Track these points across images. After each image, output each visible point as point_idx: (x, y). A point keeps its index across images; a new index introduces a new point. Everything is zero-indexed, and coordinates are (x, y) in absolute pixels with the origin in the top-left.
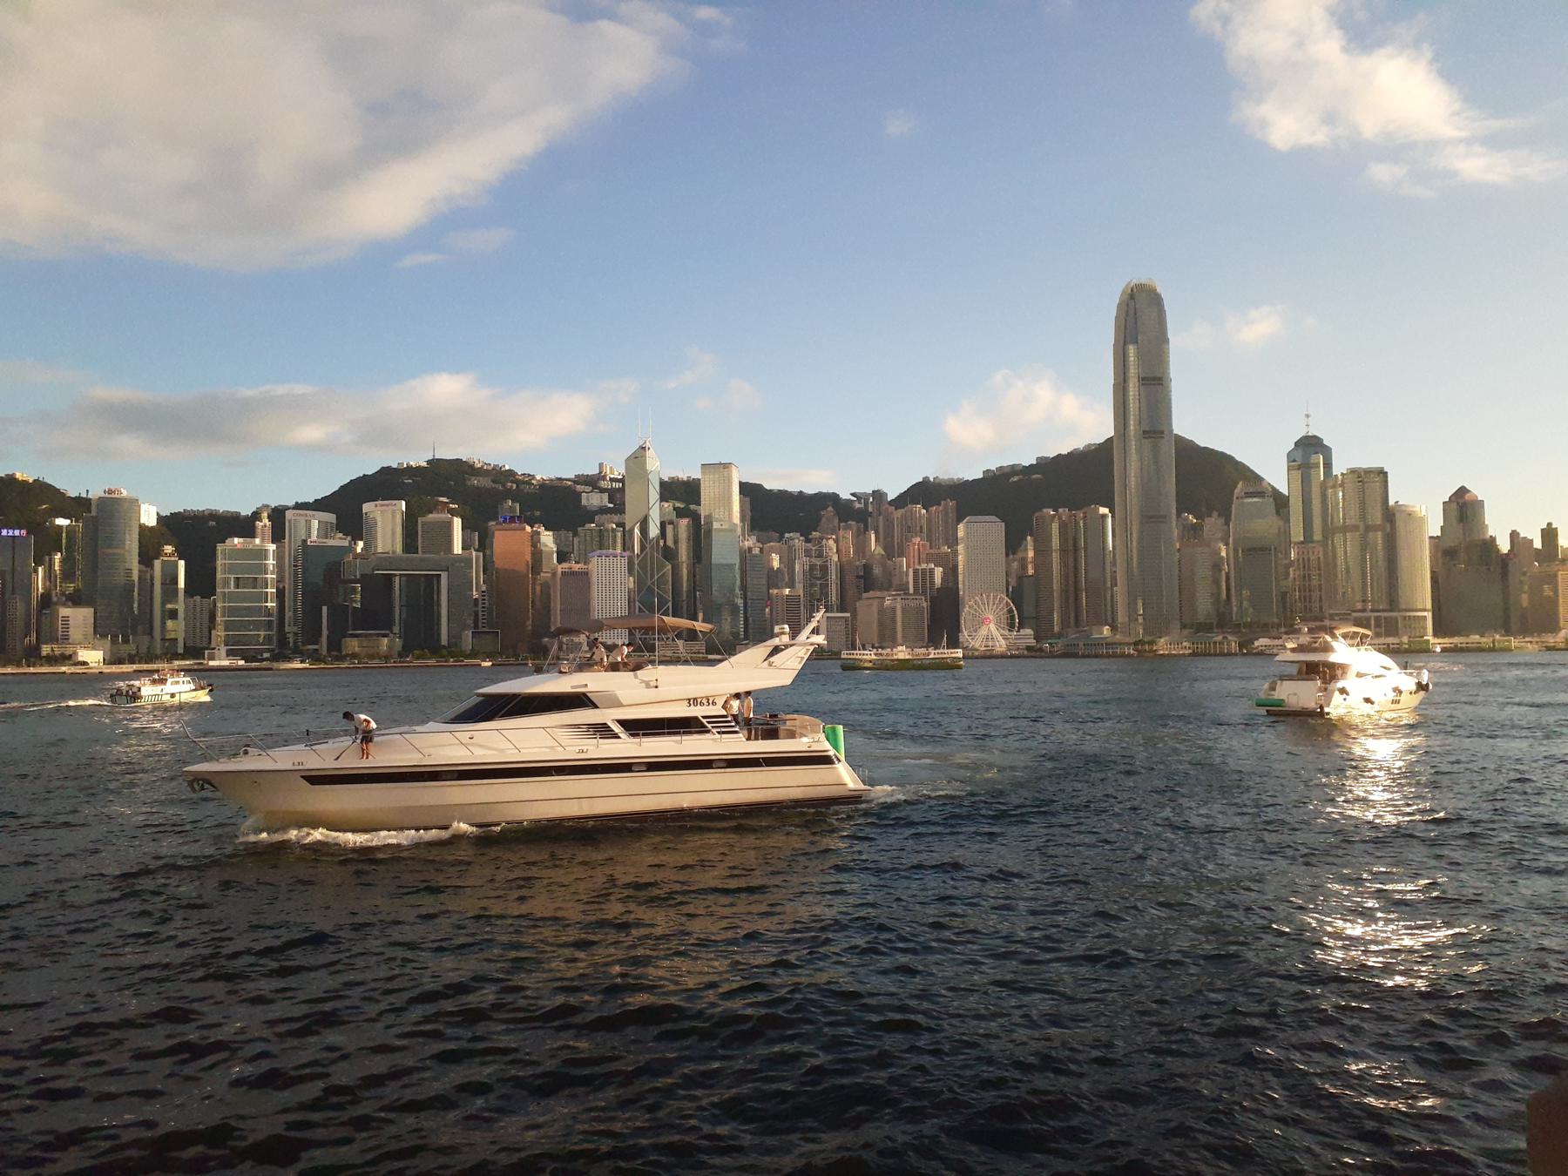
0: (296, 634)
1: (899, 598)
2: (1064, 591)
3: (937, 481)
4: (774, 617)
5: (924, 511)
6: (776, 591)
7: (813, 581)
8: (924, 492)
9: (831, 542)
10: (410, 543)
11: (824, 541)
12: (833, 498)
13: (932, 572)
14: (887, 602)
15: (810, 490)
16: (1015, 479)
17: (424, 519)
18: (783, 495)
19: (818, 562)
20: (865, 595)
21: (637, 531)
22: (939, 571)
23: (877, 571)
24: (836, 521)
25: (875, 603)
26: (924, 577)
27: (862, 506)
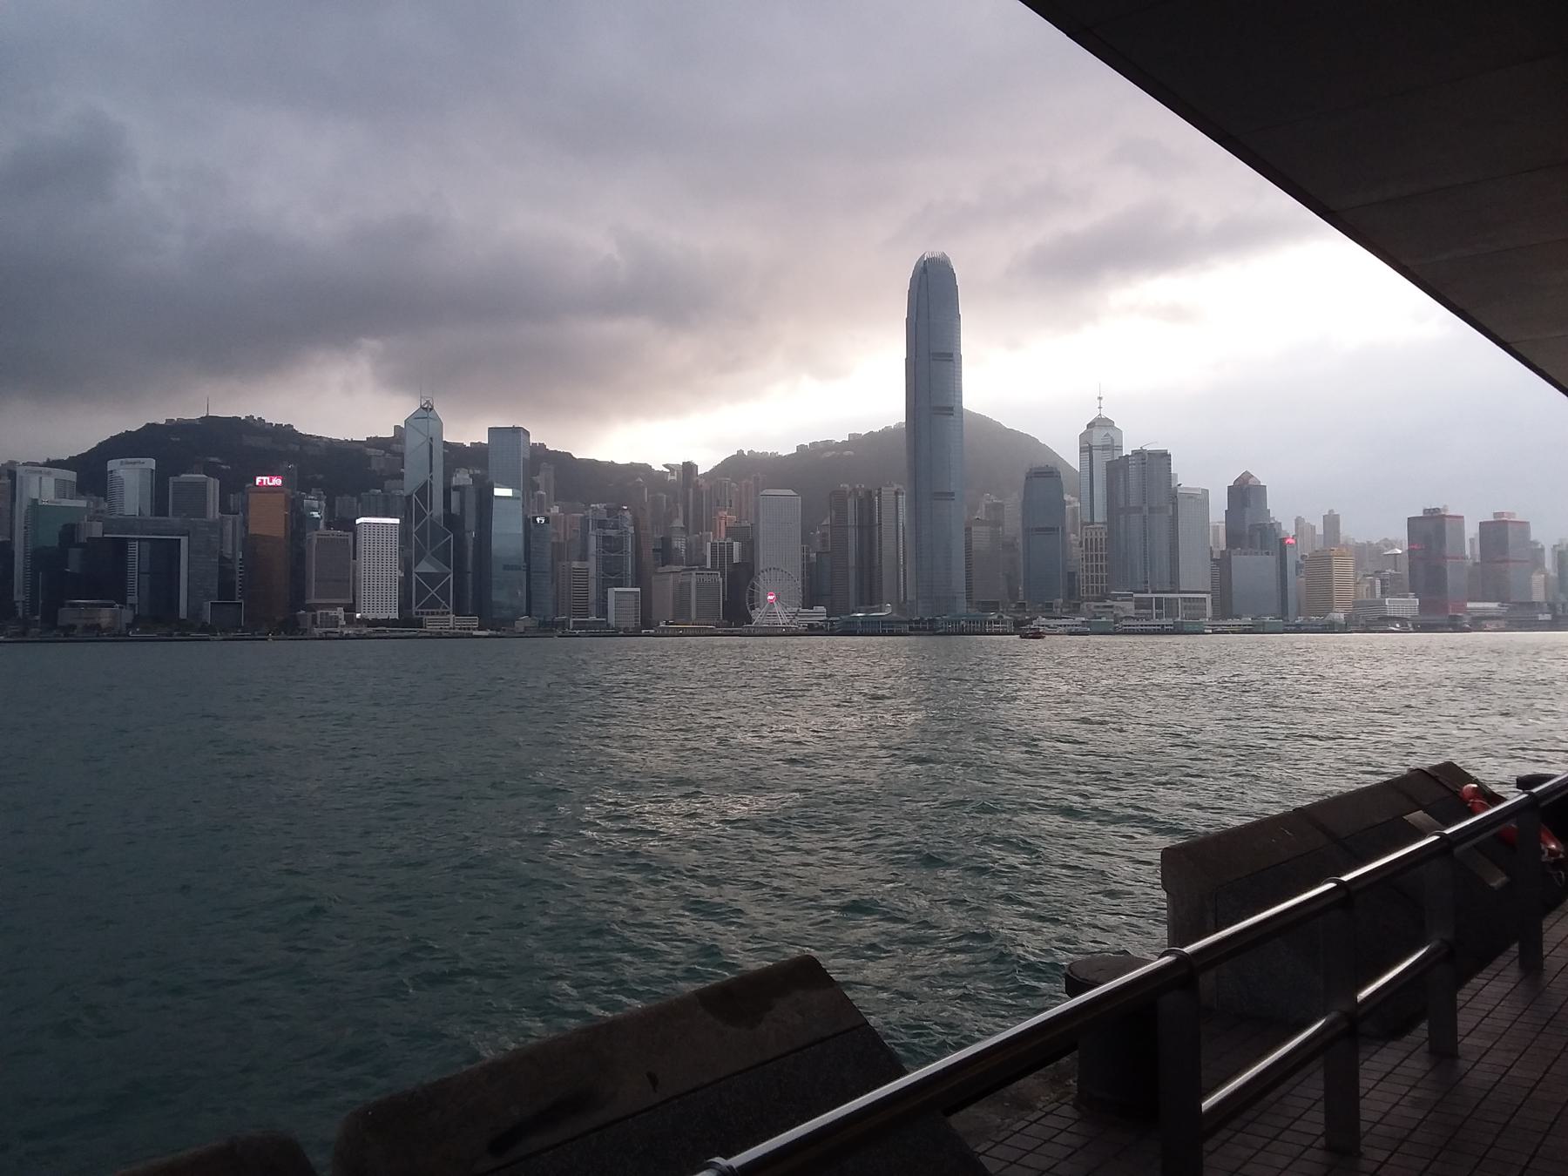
0: (23, 602)
1: (694, 573)
10: (160, 506)
13: (730, 546)
17: (175, 479)
20: (660, 569)
23: (679, 543)
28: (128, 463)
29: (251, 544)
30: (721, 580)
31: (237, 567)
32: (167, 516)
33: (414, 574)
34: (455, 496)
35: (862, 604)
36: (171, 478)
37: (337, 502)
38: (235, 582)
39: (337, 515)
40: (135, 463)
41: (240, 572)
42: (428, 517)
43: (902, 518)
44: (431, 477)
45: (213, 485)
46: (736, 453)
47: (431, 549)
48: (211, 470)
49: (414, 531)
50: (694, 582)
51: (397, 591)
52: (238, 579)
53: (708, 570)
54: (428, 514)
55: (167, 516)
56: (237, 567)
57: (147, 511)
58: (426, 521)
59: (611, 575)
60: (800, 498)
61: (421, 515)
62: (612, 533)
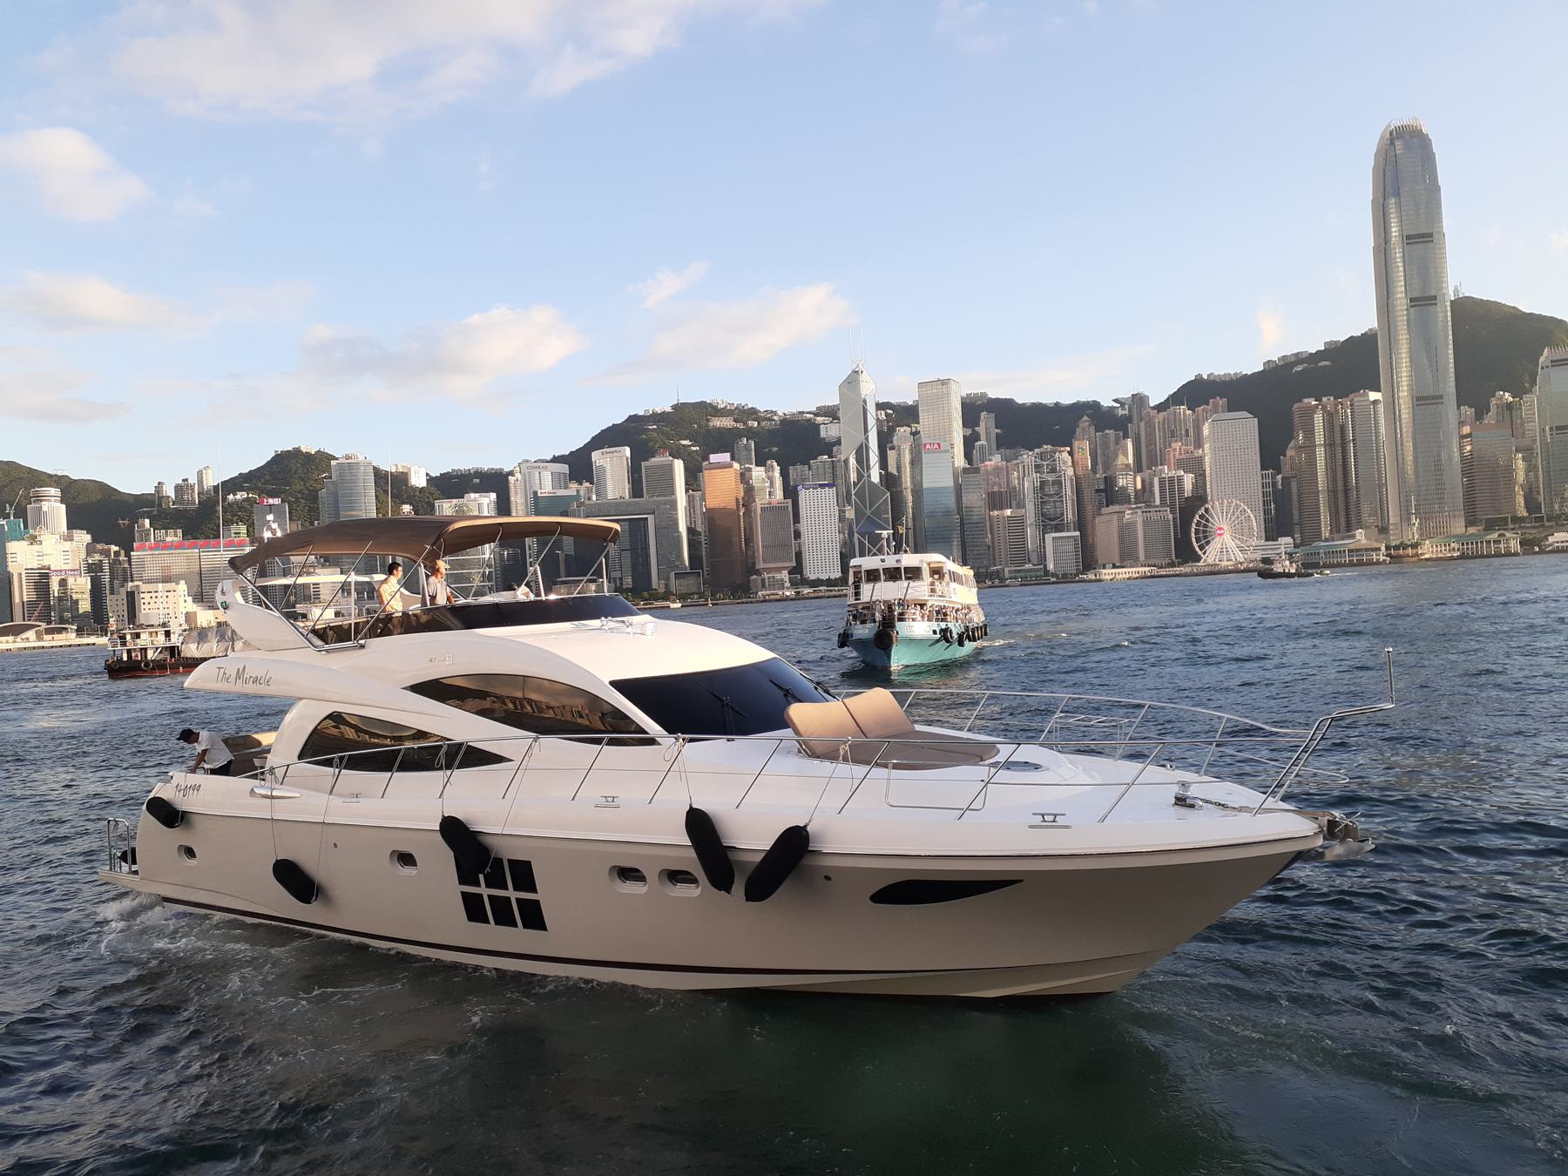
1: (1139, 511)
2: (1332, 492)
3: (1212, 378)
4: (996, 542)
5: (1189, 412)
6: (996, 513)
7: (1046, 498)
8: (1197, 393)
9: (1065, 455)
11: (1057, 455)
12: (1092, 409)
13: (1180, 479)
14: (1127, 517)
15: (1067, 400)
16: (1299, 368)
18: (1038, 409)
19: (1050, 478)
20: (1105, 510)
21: (852, 461)
22: (1188, 480)
24: (1092, 429)
25: (1115, 517)
26: (1172, 485)
27: (1126, 412)
28: (607, 453)
29: (712, 516)
30: (1171, 517)
31: (703, 538)
32: (643, 497)
35: (1338, 531)
36: (643, 463)
40: (612, 452)
43: (1383, 430)
45: (679, 466)
46: (1194, 378)
47: (871, 507)
49: (853, 493)
50: (1139, 520)
53: (1157, 507)
54: (866, 475)
55: (643, 497)
56: (703, 538)
59: (1050, 522)
60: (1256, 419)
62: (1050, 478)
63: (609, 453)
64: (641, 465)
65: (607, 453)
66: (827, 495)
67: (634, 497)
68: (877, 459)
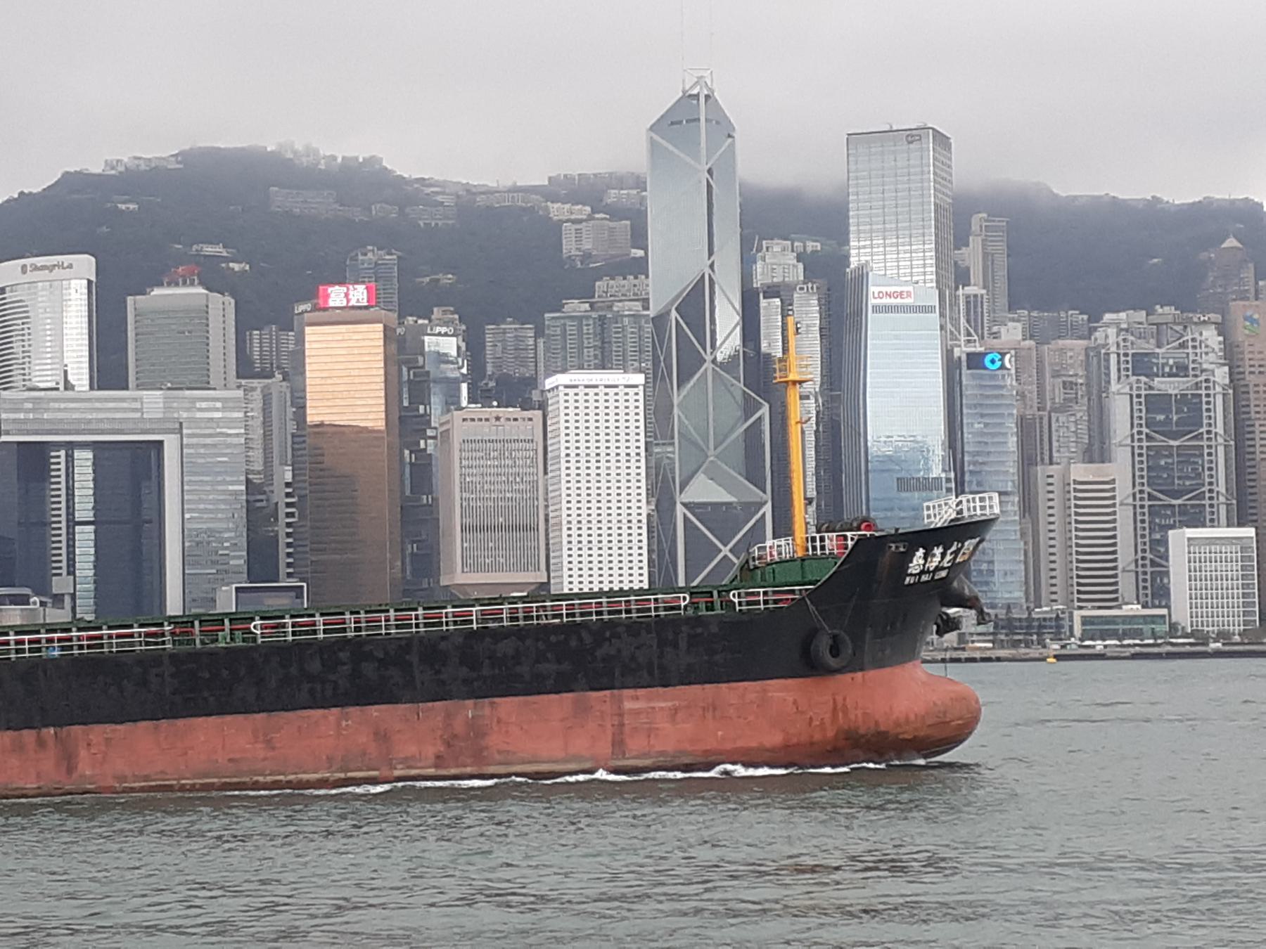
33: (680, 510)
34: (770, 308)
36: (130, 299)
37: (489, 338)
38: (277, 535)
39: (490, 369)
41: (289, 515)
42: (708, 365)
44: (712, 266)
45: (222, 308)
48: (213, 279)
49: (676, 402)
51: (645, 551)
52: (282, 530)
54: (708, 358)
55: (126, 388)
57: (80, 376)
58: (706, 370)
61: (690, 364)
63: (43, 268)
64: (125, 302)
65: (36, 268)
66: (602, 404)
67: (100, 388)
68: (737, 318)
